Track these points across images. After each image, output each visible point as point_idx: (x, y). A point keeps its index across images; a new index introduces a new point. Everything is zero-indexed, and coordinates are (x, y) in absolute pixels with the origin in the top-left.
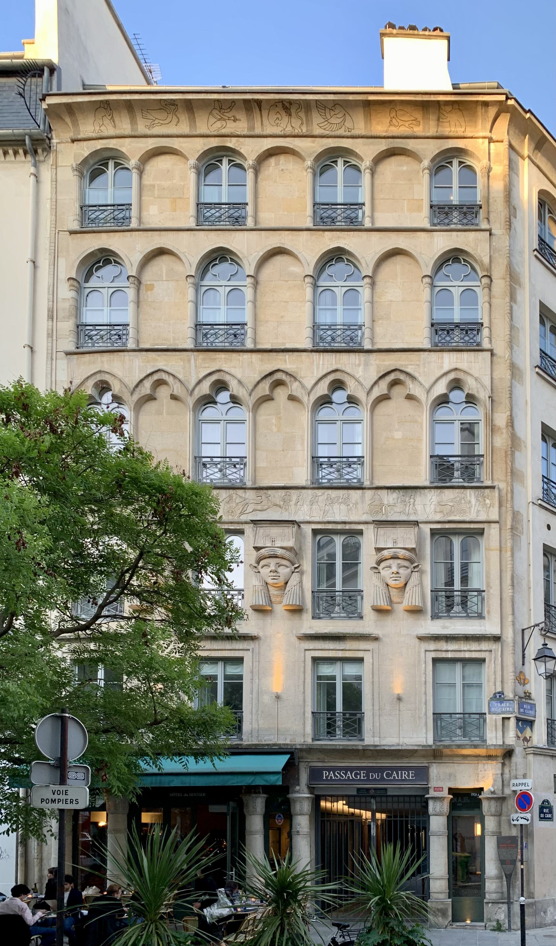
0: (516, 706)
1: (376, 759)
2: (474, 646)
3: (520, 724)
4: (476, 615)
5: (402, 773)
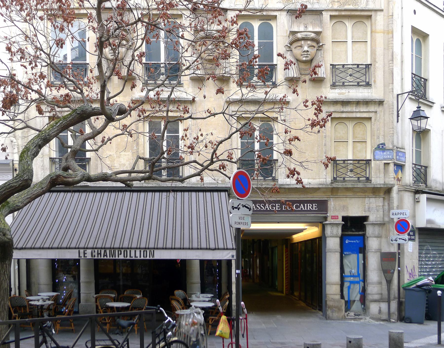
0: (395, 154)
2: (363, 109)
4: (364, 83)
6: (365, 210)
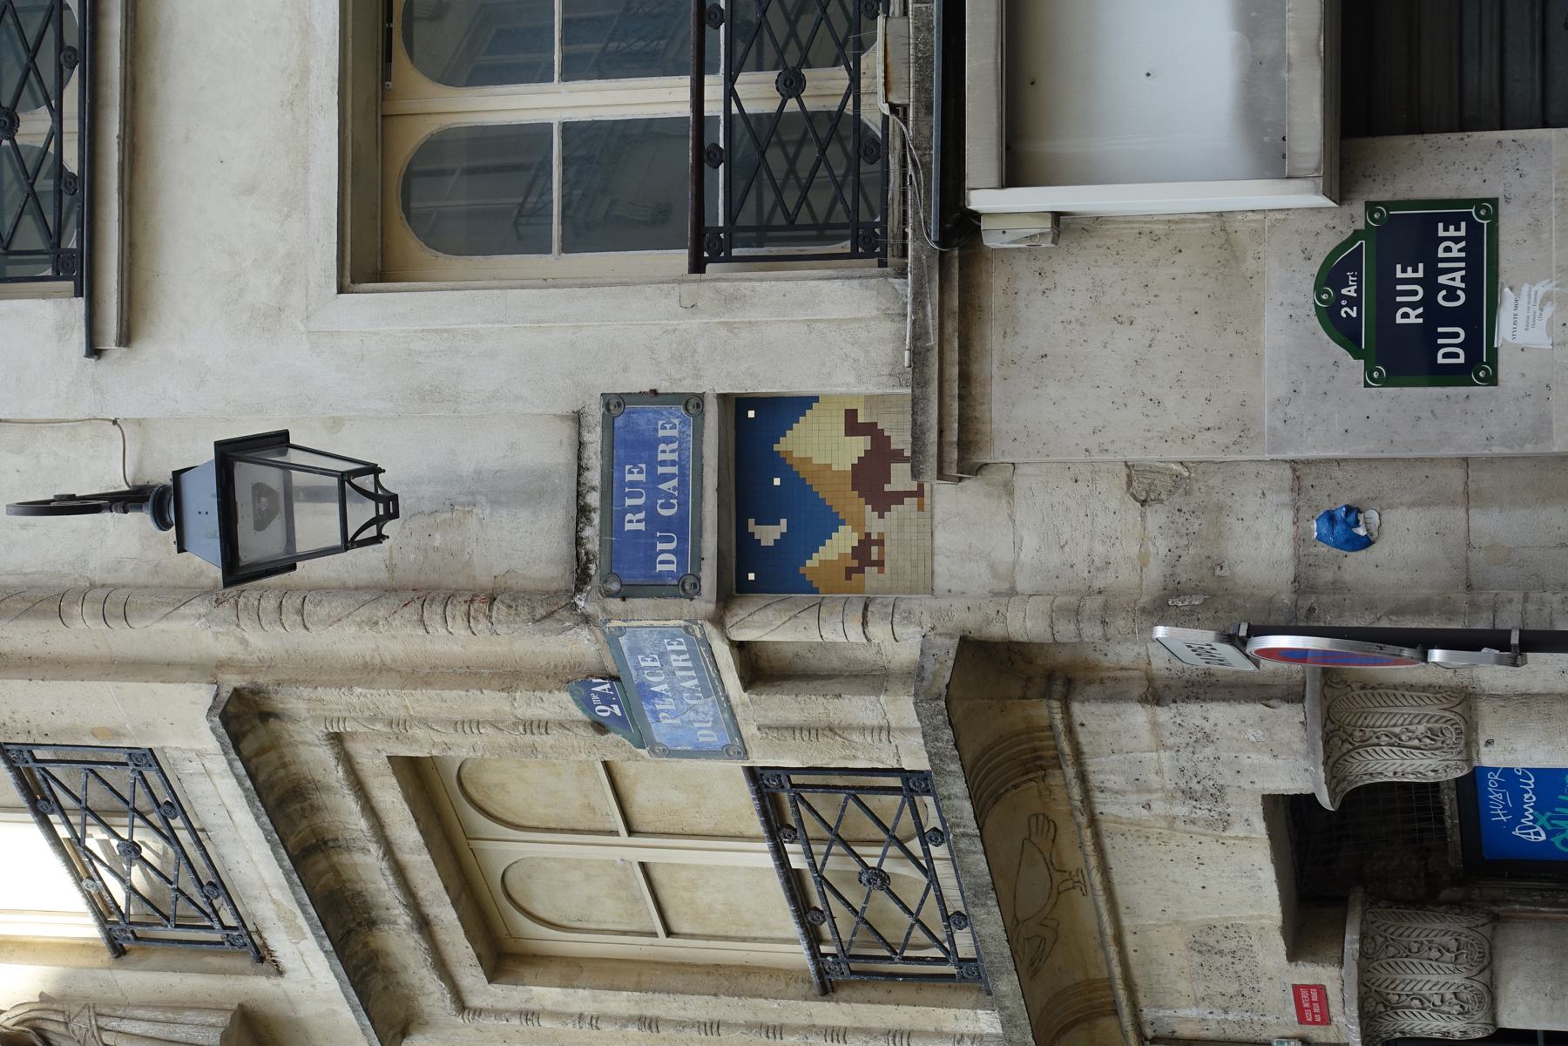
3: (768, 535)
6: (1209, 824)
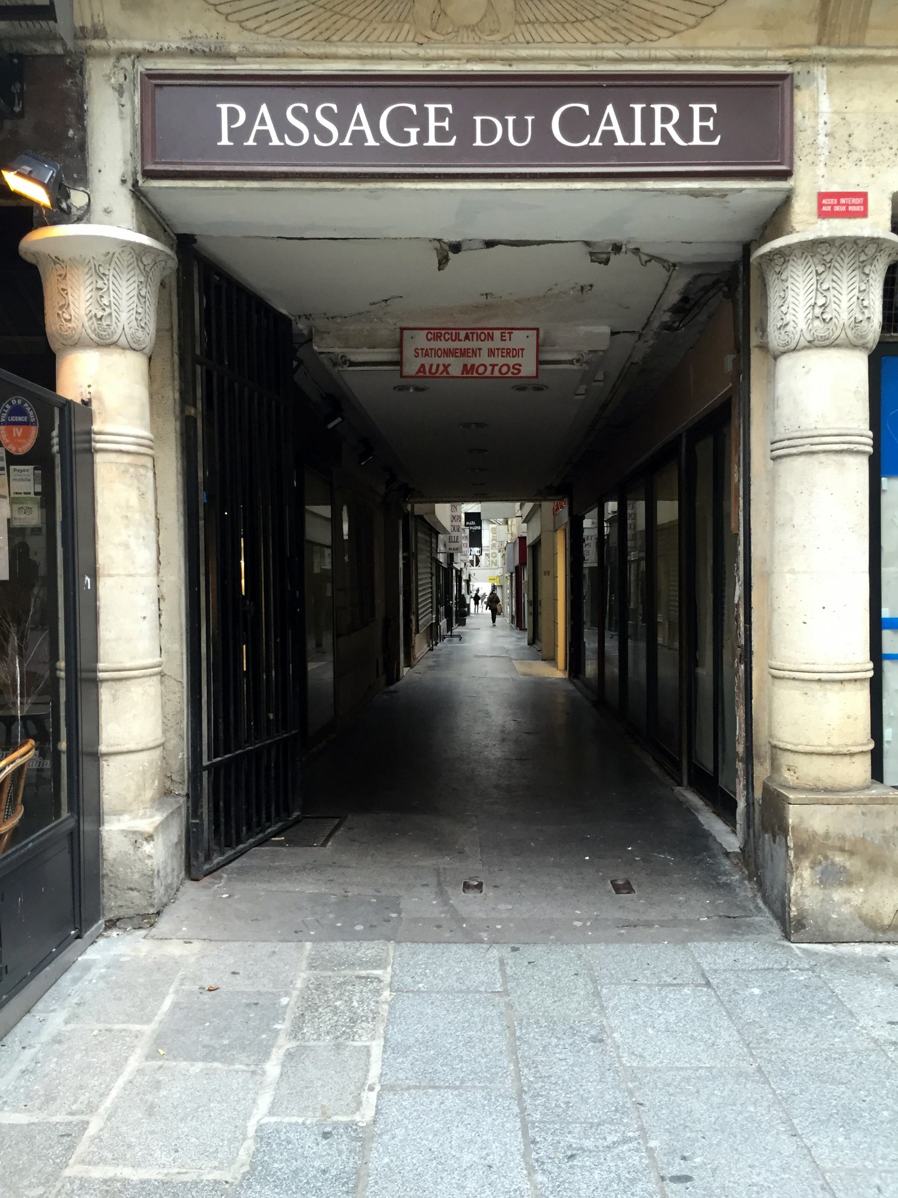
1: (504, 42)
5: (648, 115)
